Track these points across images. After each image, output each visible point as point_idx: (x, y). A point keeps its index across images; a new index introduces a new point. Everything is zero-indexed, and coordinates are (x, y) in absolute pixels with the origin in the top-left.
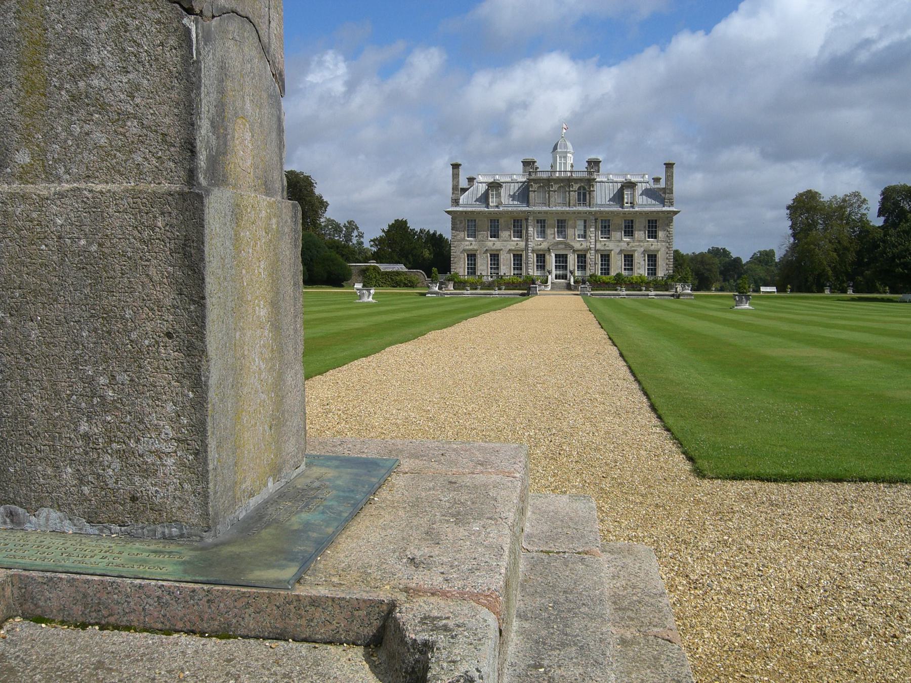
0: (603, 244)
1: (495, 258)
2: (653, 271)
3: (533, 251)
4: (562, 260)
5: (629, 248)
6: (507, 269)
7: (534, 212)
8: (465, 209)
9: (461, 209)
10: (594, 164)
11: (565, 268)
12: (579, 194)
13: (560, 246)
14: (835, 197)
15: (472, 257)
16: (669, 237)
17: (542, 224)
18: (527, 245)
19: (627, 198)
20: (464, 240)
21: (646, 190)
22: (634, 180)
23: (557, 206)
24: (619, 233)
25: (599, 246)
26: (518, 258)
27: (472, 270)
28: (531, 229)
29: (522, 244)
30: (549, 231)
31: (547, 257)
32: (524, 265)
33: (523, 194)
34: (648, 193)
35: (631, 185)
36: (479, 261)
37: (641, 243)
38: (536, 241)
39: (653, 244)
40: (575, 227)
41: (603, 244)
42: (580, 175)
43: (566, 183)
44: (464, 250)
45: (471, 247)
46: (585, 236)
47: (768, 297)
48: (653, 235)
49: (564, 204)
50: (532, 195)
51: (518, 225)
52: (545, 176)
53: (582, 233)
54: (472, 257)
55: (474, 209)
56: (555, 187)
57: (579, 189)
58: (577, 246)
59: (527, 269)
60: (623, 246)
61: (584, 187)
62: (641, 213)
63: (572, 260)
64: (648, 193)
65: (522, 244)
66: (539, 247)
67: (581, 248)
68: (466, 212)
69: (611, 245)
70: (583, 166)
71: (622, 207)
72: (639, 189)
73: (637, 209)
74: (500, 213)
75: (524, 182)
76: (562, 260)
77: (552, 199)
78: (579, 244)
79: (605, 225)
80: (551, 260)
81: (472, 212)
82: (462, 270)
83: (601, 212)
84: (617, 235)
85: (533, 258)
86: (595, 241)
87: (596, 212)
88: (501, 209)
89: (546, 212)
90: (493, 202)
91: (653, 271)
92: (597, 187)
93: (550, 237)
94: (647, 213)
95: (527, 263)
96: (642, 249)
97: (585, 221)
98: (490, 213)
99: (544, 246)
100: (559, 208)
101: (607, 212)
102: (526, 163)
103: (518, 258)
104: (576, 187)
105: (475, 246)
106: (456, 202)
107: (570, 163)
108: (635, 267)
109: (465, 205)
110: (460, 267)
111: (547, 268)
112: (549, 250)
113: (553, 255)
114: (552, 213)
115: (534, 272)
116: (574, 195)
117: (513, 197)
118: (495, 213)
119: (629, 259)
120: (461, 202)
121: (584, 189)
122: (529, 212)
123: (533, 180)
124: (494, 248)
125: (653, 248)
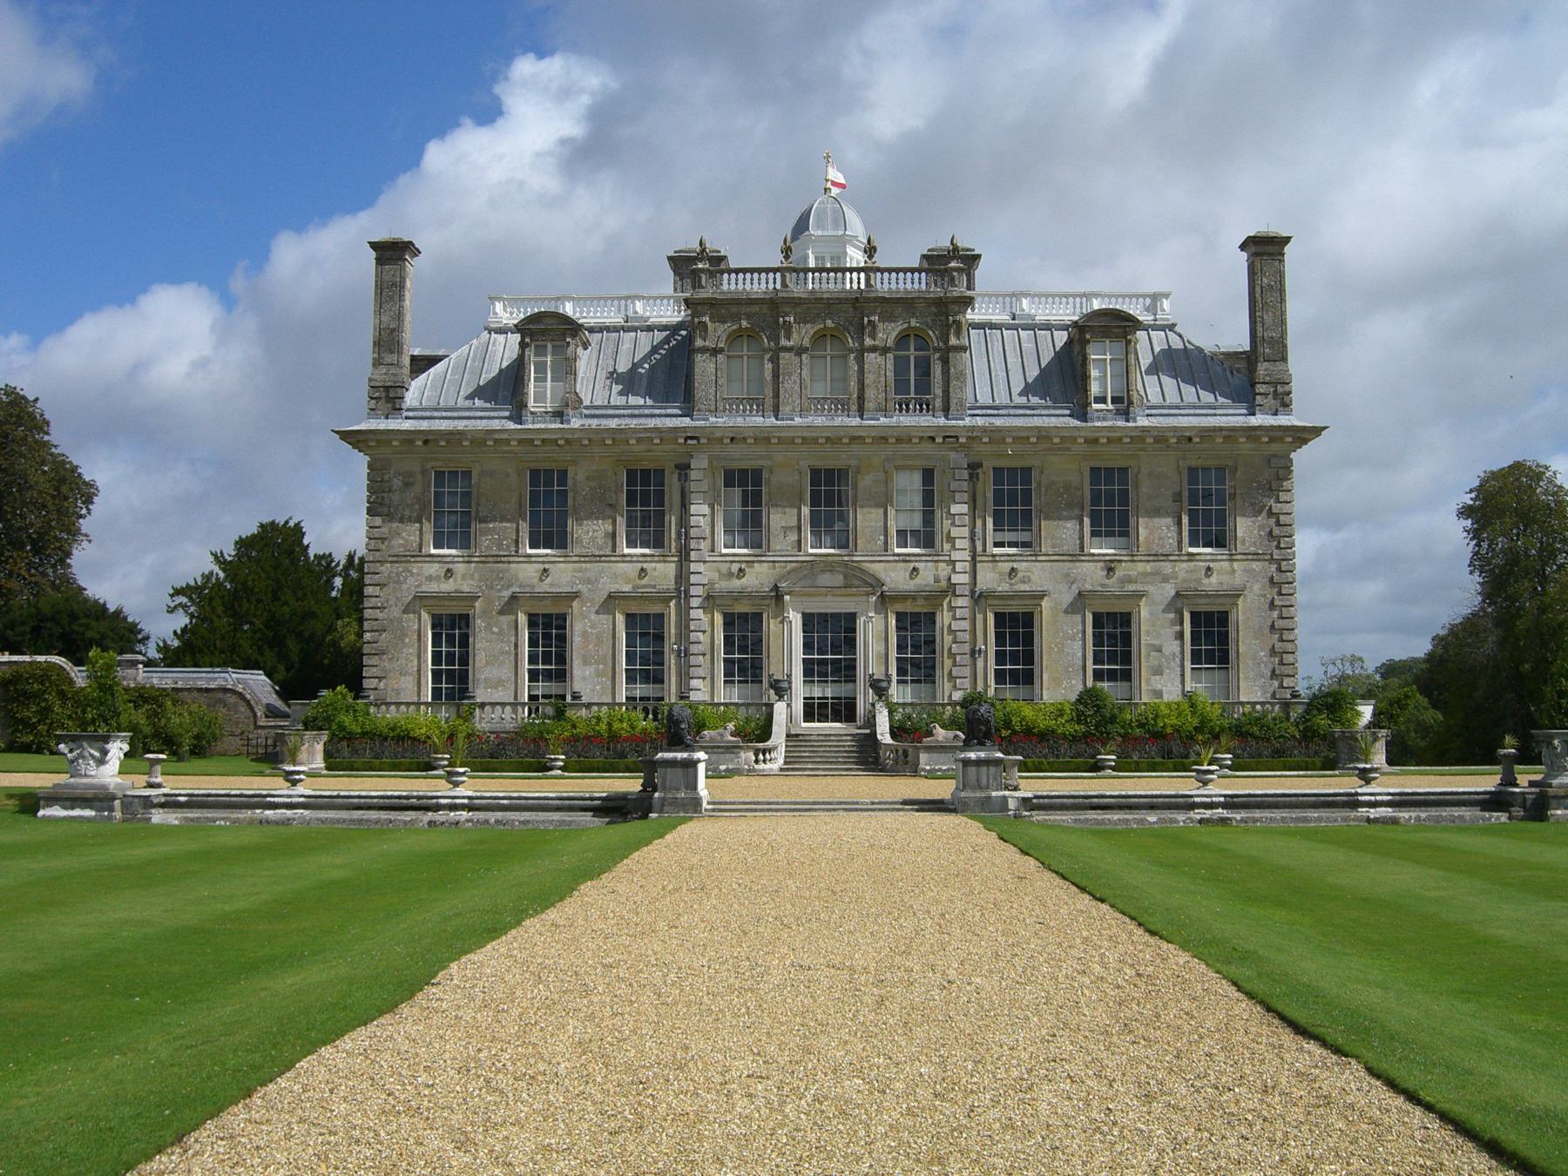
0: (1005, 570)
1: (550, 634)
3: (710, 601)
4: (832, 641)
6: (599, 680)
7: (713, 438)
9: (407, 425)
11: (846, 671)
12: (901, 366)
13: (826, 579)
15: (453, 629)
16: (1279, 539)
17: (748, 490)
18: (682, 576)
19: (1100, 380)
20: (419, 555)
21: (1169, 352)
23: (809, 408)
24: (1071, 525)
25: (988, 578)
27: (454, 681)
28: (699, 509)
29: (664, 573)
30: (778, 519)
31: (771, 626)
32: (671, 662)
33: (670, 371)
38: (719, 556)
39: (1216, 572)
40: (884, 501)
41: (1005, 570)
43: (846, 318)
44: (421, 599)
45: (447, 586)
46: (926, 538)
49: (842, 406)
50: (704, 367)
51: (650, 497)
52: (758, 287)
53: (916, 522)
54: (453, 629)
55: (461, 425)
56: (802, 334)
57: (902, 339)
58: (895, 578)
59: (684, 676)
60: (1091, 575)
61: (929, 314)
62: (1160, 437)
63: (876, 640)
66: (736, 584)
67: (912, 585)
68: (429, 438)
69: (1037, 575)
71: (1082, 413)
72: (1146, 346)
73: (1142, 422)
74: (572, 441)
75: (674, 329)
76: (832, 641)
77: (789, 385)
78: (903, 569)
79: (1014, 500)
80: (788, 644)
81: (453, 437)
82: (408, 683)
83: (997, 436)
84: (1061, 532)
86: (970, 561)
87: (974, 435)
88: (576, 423)
89: (763, 438)
90: (540, 394)
93: (781, 543)
94: (1186, 437)
95: (684, 654)
96: (1169, 590)
97: (928, 476)
98: (526, 441)
99: (759, 577)
100: (819, 421)
101: (1021, 437)
102: (684, 266)
103: (648, 635)
104: (888, 333)
105: (464, 580)
106: (388, 397)
107: (868, 245)
108: (1144, 662)
109: (420, 413)
110: (403, 679)
111: (773, 669)
112: (777, 596)
113: (796, 619)
114: (787, 440)
115: (710, 688)
117: (628, 382)
120: (411, 398)
121: (923, 344)
122: (691, 436)
123: (712, 304)
124: (545, 587)
125: (1212, 584)
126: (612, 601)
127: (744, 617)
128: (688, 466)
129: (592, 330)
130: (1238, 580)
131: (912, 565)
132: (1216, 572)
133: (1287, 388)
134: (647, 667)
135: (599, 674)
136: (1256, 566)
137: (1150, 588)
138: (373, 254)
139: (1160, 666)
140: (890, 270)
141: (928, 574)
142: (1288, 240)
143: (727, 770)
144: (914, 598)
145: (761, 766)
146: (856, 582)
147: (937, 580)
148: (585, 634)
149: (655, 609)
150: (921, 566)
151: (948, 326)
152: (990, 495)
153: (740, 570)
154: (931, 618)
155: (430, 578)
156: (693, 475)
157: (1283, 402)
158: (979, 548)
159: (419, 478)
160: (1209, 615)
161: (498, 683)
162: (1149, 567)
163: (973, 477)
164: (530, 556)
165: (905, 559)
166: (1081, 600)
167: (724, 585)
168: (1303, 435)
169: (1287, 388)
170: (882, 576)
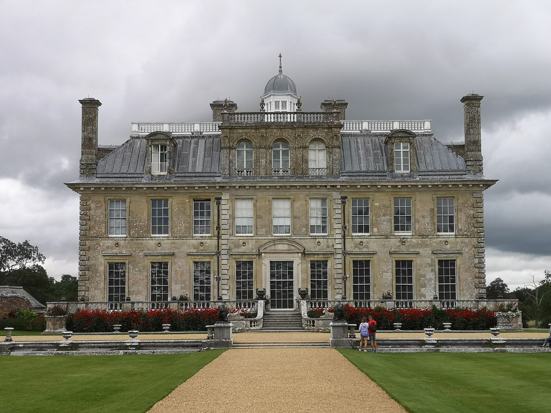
9: (97, 181)
25: (349, 247)
45: (116, 251)
53: (319, 223)
58: (310, 245)
60: (393, 243)
66: (242, 249)
67: (317, 249)
85: (228, 268)
96: (429, 251)
99: (251, 247)
112: (259, 255)
120: (99, 170)
124: (159, 250)
127: (245, 263)
128: (221, 199)
129: (178, 138)
130: (459, 248)
131: (317, 240)
133: (480, 163)
135: (182, 288)
136: (467, 240)
137: (421, 251)
138: (81, 105)
139: (425, 284)
140: (307, 113)
142: (481, 98)
143: (239, 330)
144: (318, 254)
145: (253, 328)
146: (293, 248)
147: (328, 247)
148: (176, 271)
149: (207, 259)
150: (321, 240)
151: (333, 137)
152: (351, 210)
153: (243, 243)
154: (325, 263)
155: (108, 247)
156: (223, 202)
158: (346, 233)
159: (103, 204)
160: (447, 261)
161: (138, 293)
162: (420, 241)
163: (344, 203)
164: (152, 237)
165: (315, 238)
167: (235, 251)
169: (480, 163)
170: (304, 245)
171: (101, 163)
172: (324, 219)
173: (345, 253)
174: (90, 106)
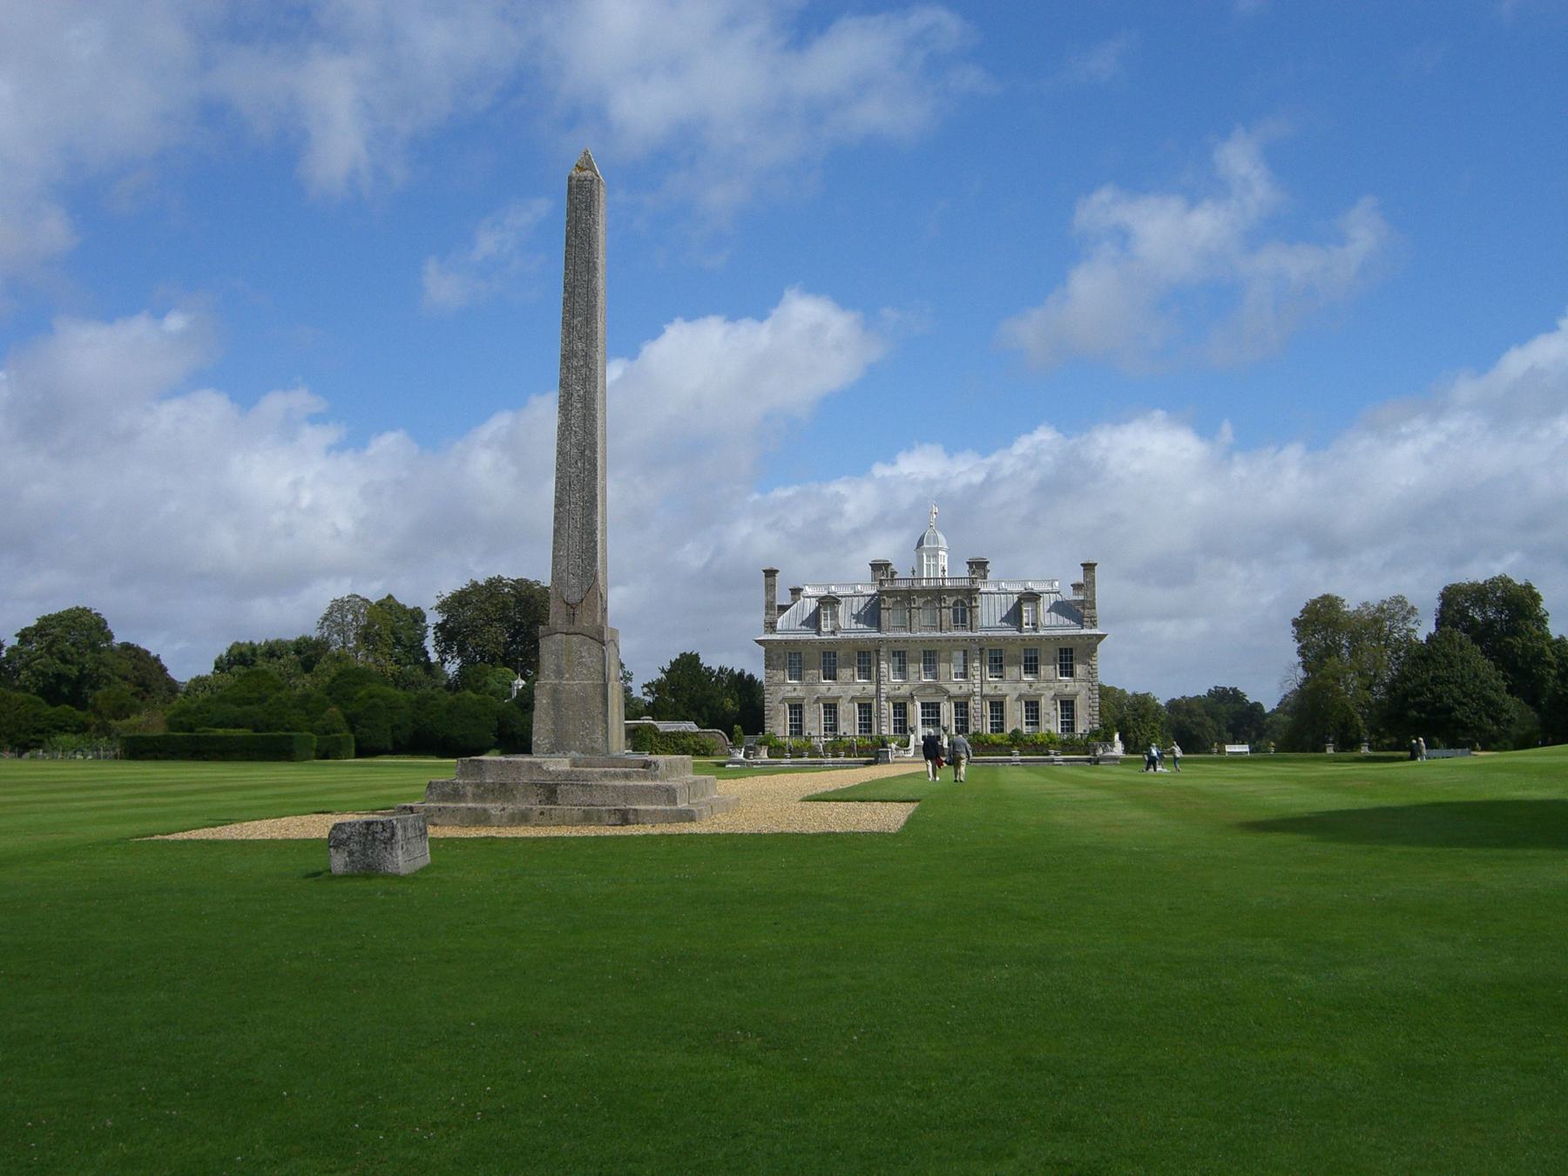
1: (831, 709)
2: (1069, 725)
3: (888, 699)
5: (1032, 692)
6: (849, 726)
7: (888, 640)
8: (785, 637)
9: (778, 637)
10: (978, 566)
11: (936, 723)
12: (955, 612)
13: (929, 691)
14: (1365, 604)
15: (796, 708)
16: (1092, 673)
17: (901, 658)
18: (878, 690)
19: (1027, 617)
21: (1057, 603)
22: (1037, 588)
23: (923, 631)
24: (1016, 669)
25: (987, 690)
26: (865, 708)
27: (797, 728)
28: (884, 665)
29: (872, 688)
30: (912, 668)
31: (910, 707)
32: (874, 720)
33: (872, 614)
34: (1061, 608)
35: (1032, 597)
36: (807, 716)
37: (1049, 683)
38: (892, 683)
39: (1068, 685)
40: (950, 662)
42: (958, 584)
44: (785, 699)
46: (965, 675)
47: (1237, 759)
48: (1067, 670)
49: (934, 628)
50: (884, 614)
51: (865, 659)
52: (903, 586)
54: (796, 708)
55: (798, 637)
56: (919, 602)
57: (955, 604)
58: (954, 690)
59: (879, 725)
60: (1024, 688)
62: (1048, 638)
63: (947, 712)
64: (1061, 608)
65: (872, 688)
68: (786, 642)
70: (964, 571)
72: (1046, 602)
73: (1042, 633)
76: (932, 711)
77: (915, 621)
78: (956, 686)
80: (916, 713)
81: (796, 642)
82: (781, 729)
83: (988, 638)
84: (1013, 671)
85: (888, 709)
86: (981, 682)
89: (906, 640)
90: (826, 625)
91: (1069, 725)
92: (982, 601)
93: (913, 677)
94: (1057, 638)
98: (822, 642)
99: (905, 690)
100: (926, 634)
101: (998, 639)
102: (878, 567)
104: (950, 601)
105: (800, 692)
106: (771, 626)
107: (943, 566)
108: (1042, 720)
109: (784, 631)
110: (779, 725)
111: (910, 724)
113: (918, 704)
114: (915, 641)
116: (948, 614)
117: (858, 618)
118: (830, 642)
119: (1033, 708)
120: (779, 626)
121: (963, 604)
122: (880, 640)
123: (886, 592)
126: (853, 699)
132: (1068, 685)
134: (866, 725)
141: (965, 688)
157: (1094, 624)
166: (1020, 698)
168: (1101, 637)
171: (780, 620)
172: (966, 668)
173: (983, 697)
174: (770, 573)
